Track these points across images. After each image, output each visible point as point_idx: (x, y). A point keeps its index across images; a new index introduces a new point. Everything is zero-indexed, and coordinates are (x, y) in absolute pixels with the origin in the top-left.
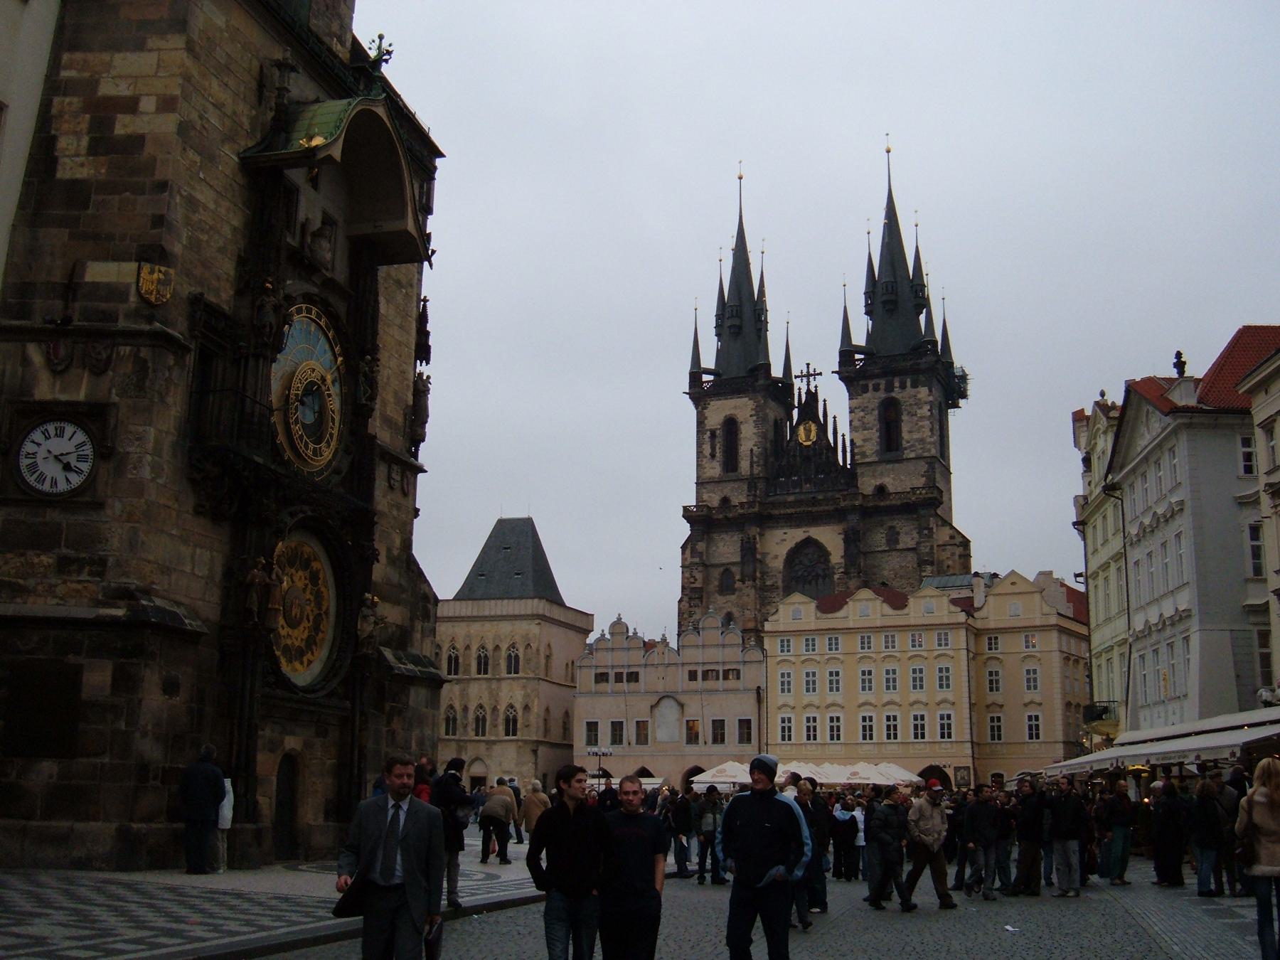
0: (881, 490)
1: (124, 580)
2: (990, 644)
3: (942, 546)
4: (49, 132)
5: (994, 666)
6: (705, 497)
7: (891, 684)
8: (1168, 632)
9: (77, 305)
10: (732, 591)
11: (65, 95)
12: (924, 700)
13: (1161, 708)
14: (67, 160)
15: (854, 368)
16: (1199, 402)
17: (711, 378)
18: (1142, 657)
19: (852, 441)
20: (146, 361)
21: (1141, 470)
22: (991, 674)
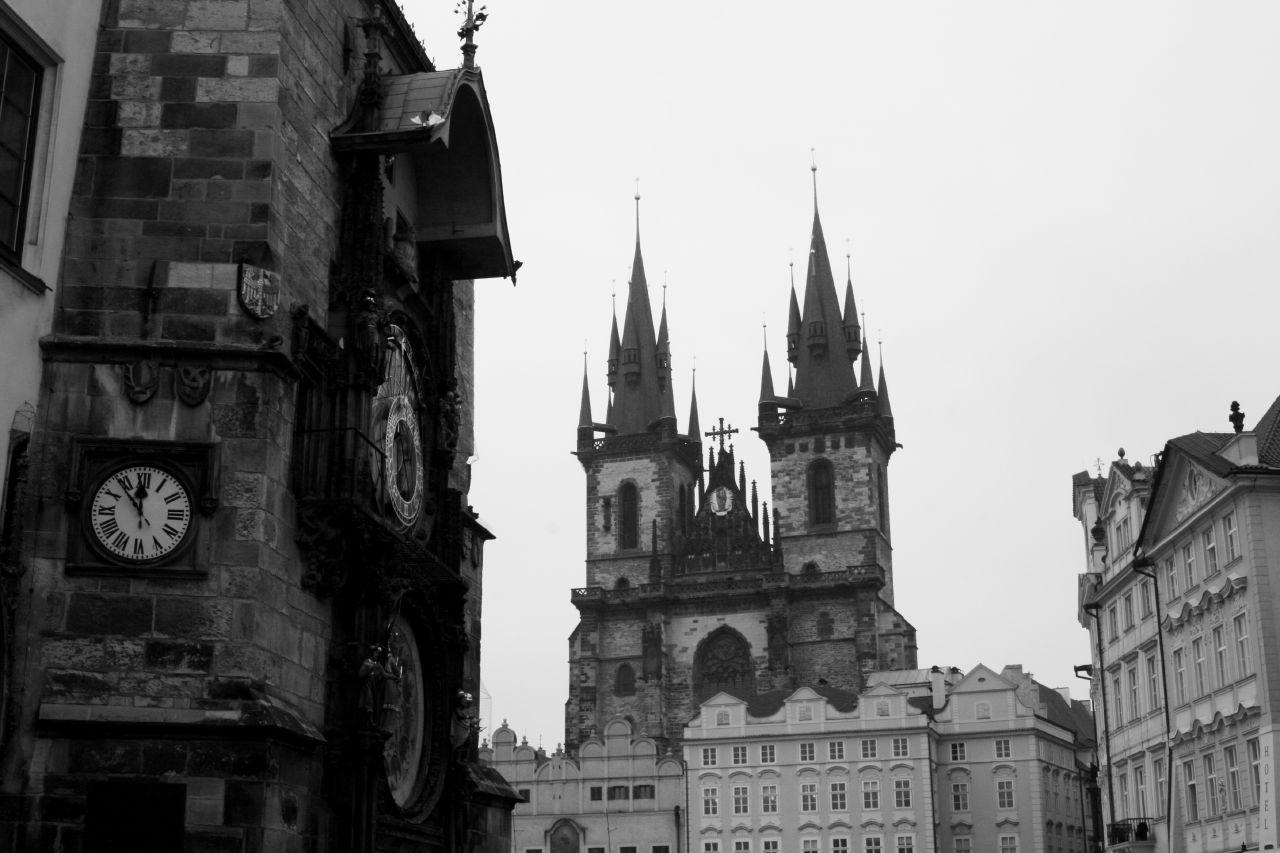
0: (811, 569)
2: (955, 752)
3: (886, 636)
4: (108, 97)
5: (960, 779)
6: (598, 577)
7: (839, 801)
8: (1227, 733)
9: (160, 317)
11: (126, 50)
12: (879, 820)
13: (1218, 826)
14: (134, 133)
15: (778, 424)
16: (1260, 461)
18: (1188, 765)
19: (776, 512)
20: (253, 391)
21: (1183, 543)
22: (956, 787)
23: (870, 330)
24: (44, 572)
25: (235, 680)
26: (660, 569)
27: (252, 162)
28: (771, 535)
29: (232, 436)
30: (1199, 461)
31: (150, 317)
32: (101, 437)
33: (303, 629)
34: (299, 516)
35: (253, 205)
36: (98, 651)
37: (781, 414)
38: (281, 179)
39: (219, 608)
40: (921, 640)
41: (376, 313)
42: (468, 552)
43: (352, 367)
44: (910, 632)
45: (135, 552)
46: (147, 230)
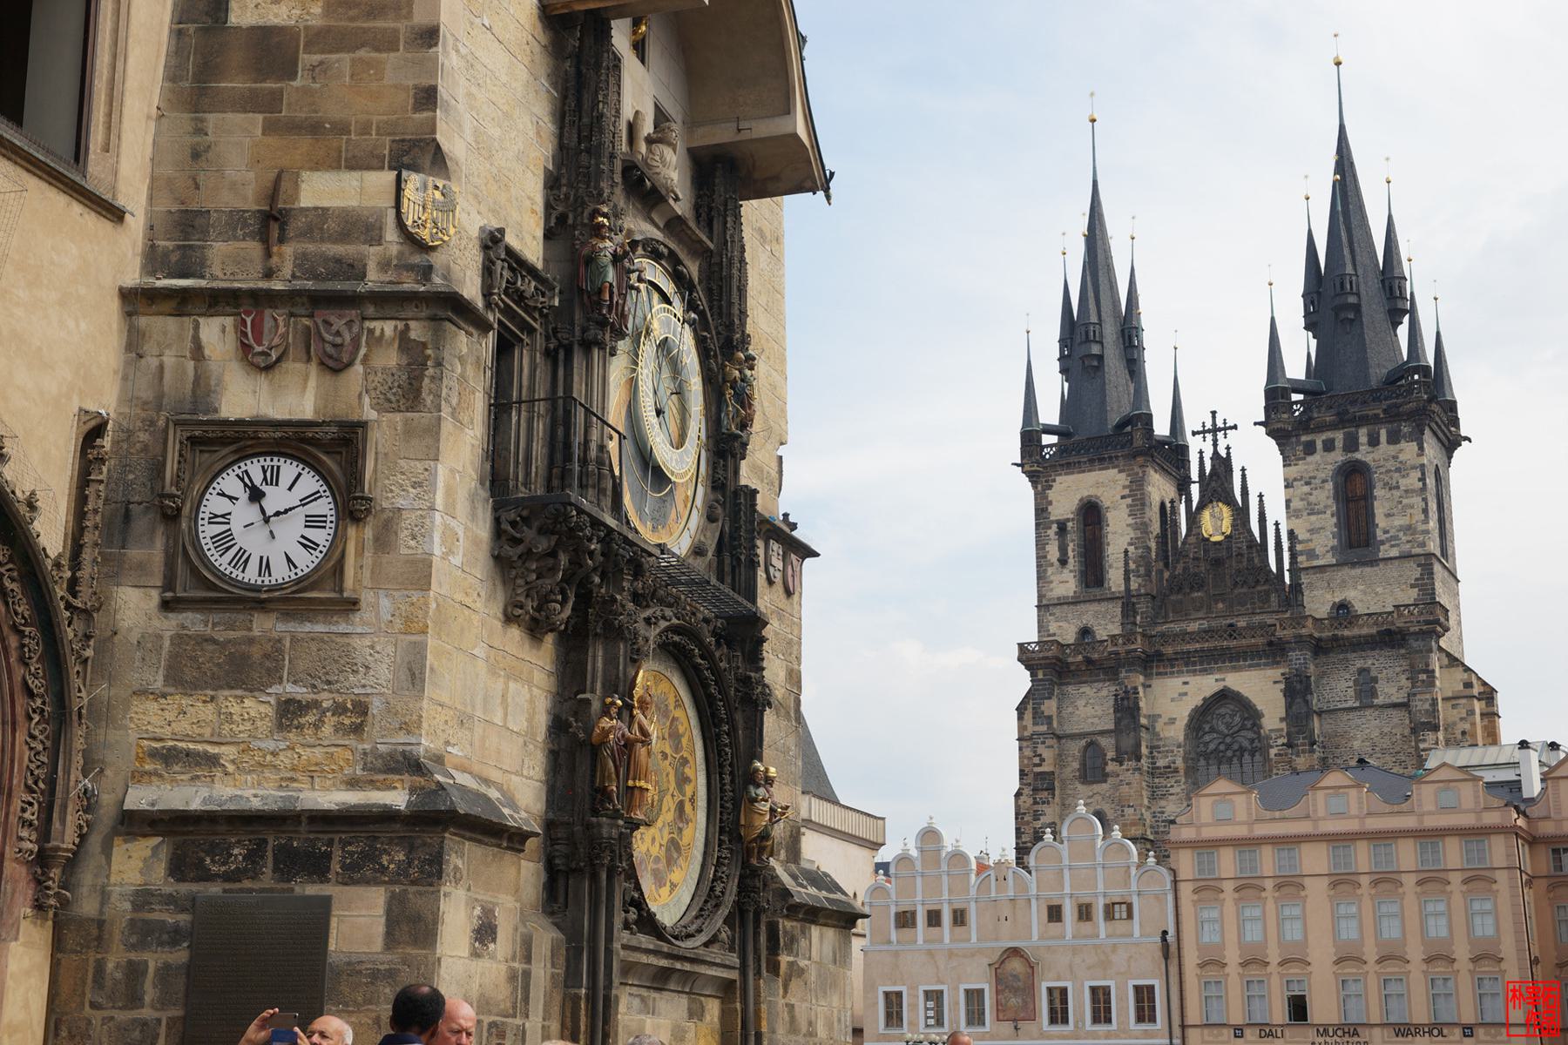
9: (288, 250)
10: (1103, 777)
15: (1291, 415)
17: (1053, 439)
19: (1291, 533)
23: (1423, 279)
24: (134, 607)
25: (400, 748)
26: (1135, 613)
27: (413, 28)
28: (1286, 566)
29: (394, 410)
31: (275, 249)
33: (508, 678)
34: (497, 521)
35: (416, 87)
36: (207, 712)
37: (1296, 403)
38: (457, 51)
40: (1503, 703)
41: (611, 239)
42: (778, 575)
44: (1489, 695)
46: (269, 128)
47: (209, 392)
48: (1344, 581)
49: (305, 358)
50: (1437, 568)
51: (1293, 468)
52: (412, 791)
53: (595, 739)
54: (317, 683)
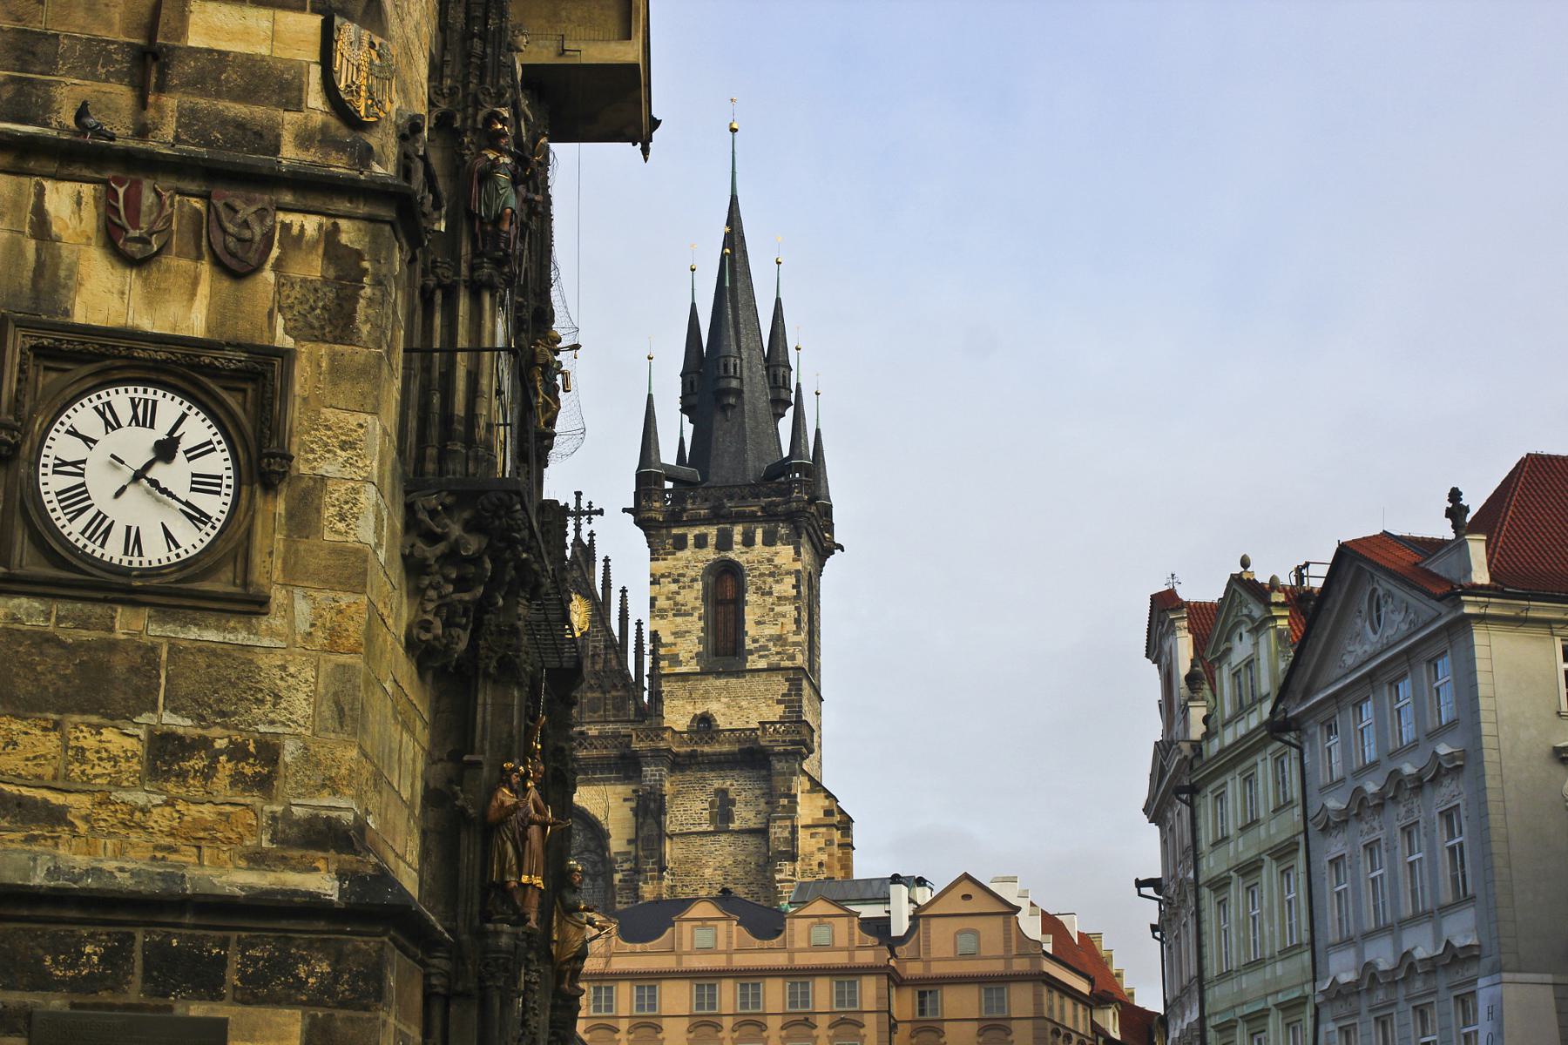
0: (704, 722)
1: (326, 800)
9: (171, 102)
15: (663, 504)
19: (655, 636)
23: (808, 369)
25: (324, 813)
28: (647, 671)
30: (1392, 574)
31: (151, 99)
32: (59, 319)
34: (409, 508)
37: (669, 491)
39: (292, 670)
43: (465, 249)
44: (846, 824)
45: (126, 553)
47: (56, 286)
48: (707, 692)
49: (193, 253)
50: (805, 684)
51: (661, 563)
52: (341, 876)
53: (493, 815)
54: (206, 712)
